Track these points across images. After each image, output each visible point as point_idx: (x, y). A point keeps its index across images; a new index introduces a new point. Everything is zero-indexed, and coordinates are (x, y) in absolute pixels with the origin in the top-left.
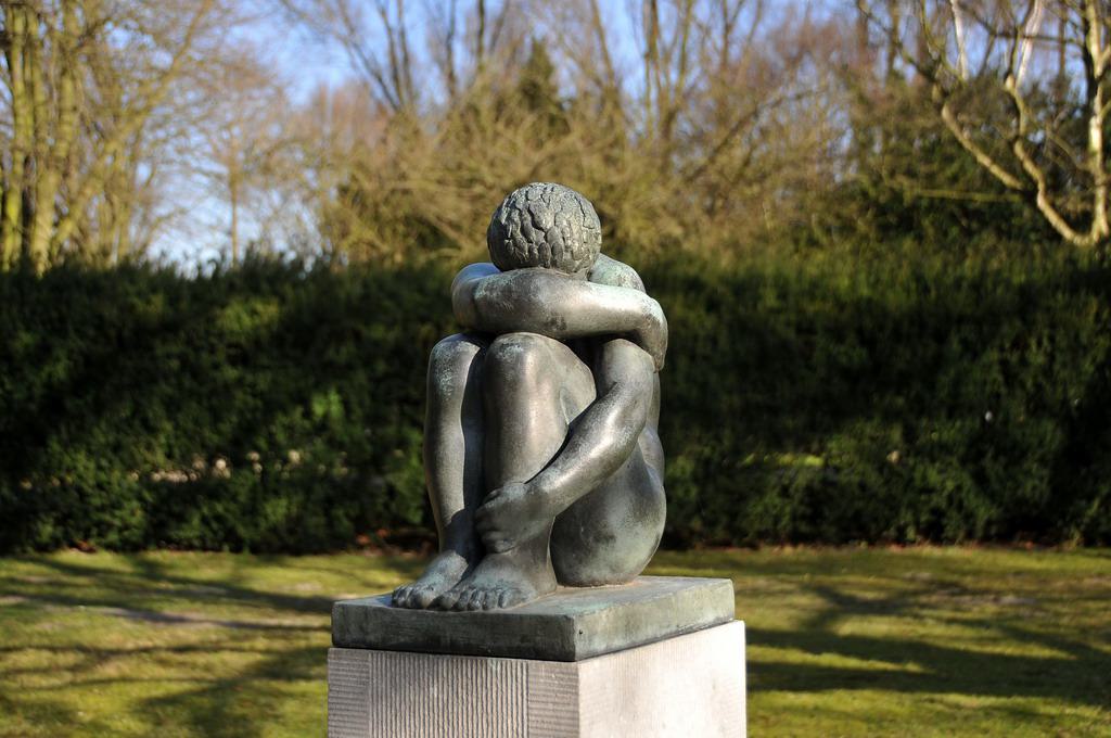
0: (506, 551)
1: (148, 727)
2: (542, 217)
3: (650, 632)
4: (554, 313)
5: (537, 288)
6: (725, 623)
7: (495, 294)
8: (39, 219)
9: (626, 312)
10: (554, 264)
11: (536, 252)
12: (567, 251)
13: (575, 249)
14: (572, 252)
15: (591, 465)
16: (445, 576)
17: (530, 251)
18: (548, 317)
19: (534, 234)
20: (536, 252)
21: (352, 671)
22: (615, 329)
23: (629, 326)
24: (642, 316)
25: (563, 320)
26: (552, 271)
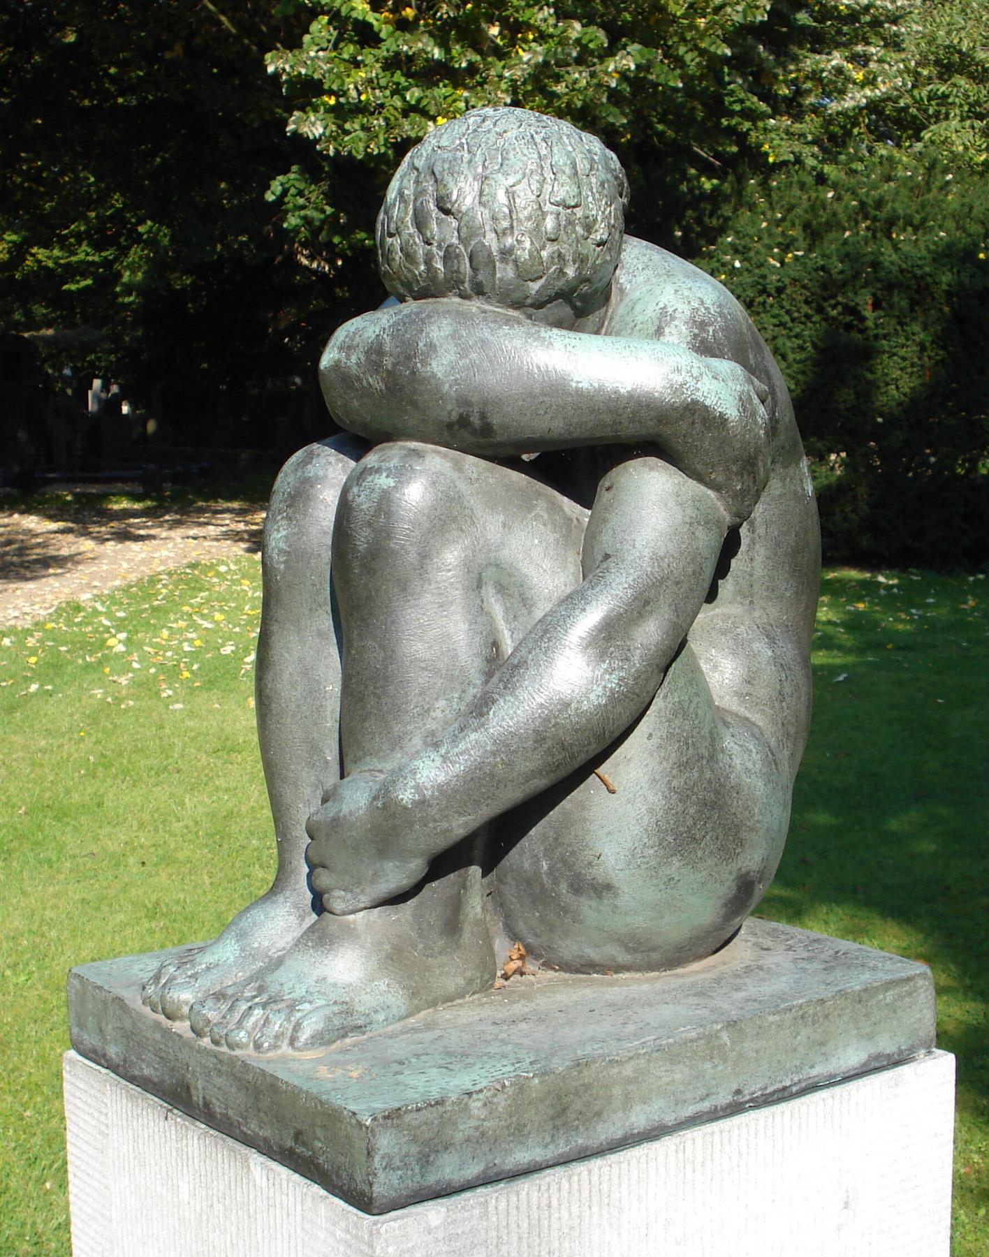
0: (354, 912)
1: (396, 1000)
2: (451, 185)
3: (639, 1119)
4: (463, 401)
5: (432, 347)
6: (897, 1063)
7: (354, 359)
8: (526, 568)
9: (630, 396)
10: (479, 290)
11: (439, 265)
12: (503, 260)
13: (523, 254)
14: (515, 261)
15: (503, 745)
16: (243, 950)
17: (428, 261)
18: (452, 411)
19: (435, 227)
20: (439, 265)
21: (90, 1106)
22: (608, 432)
23: (649, 428)
24: (673, 407)
25: (483, 416)
26: (475, 305)
